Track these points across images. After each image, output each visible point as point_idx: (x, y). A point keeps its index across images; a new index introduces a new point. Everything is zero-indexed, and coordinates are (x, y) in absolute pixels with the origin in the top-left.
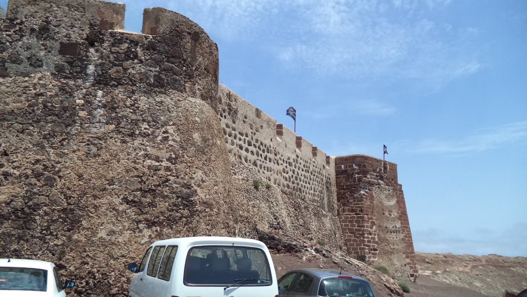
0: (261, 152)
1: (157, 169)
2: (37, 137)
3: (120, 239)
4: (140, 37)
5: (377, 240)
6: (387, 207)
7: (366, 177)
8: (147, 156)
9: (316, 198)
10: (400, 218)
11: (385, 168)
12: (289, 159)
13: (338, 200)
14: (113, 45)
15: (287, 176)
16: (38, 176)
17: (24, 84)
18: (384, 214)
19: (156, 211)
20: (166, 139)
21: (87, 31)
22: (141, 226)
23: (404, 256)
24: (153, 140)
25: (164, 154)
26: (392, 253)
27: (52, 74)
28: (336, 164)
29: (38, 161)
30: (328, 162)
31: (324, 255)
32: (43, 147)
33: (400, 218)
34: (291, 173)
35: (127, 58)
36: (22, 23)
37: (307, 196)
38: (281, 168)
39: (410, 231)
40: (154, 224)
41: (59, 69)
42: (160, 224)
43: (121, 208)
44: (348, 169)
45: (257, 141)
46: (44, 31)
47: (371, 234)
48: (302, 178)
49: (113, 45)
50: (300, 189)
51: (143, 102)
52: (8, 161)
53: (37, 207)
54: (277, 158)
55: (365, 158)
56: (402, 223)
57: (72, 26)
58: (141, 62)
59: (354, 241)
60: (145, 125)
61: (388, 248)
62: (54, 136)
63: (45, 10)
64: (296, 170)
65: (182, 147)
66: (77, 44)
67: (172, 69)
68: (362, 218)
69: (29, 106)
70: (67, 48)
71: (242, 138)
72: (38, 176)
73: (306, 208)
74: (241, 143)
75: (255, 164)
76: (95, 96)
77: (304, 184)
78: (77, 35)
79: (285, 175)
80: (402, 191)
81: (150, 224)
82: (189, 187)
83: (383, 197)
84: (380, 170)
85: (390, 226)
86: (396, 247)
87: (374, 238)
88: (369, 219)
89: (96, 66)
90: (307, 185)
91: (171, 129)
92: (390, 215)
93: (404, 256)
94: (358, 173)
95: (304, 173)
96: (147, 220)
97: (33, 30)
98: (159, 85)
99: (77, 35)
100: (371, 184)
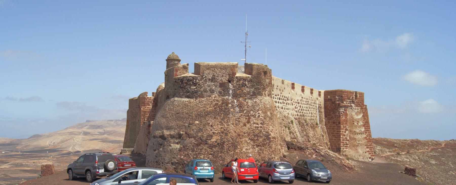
0: (284, 101)
1: (258, 128)
2: (220, 120)
3: (249, 151)
4: (246, 77)
5: (348, 139)
6: (356, 120)
7: (343, 103)
8: (254, 123)
9: (312, 118)
10: (364, 126)
11: (356, 96)
12: (298, 100)
13: (326, 116)
14: (237, 82)
16: (223, 133)
17: (210, 100)
18: (354, 124)
19: (259, 142)
20: (259, 116)
21: (228, 77)
22: (255, 147)
23: (366, 147)
24: (255, 117)
25: (259, 122)
26: (357, 146)
27: (218, 95)
28: (325, 95)
29: (222, 128)
30: (320, 95)
31: (316, 151)
32: (222, 123)
33: (364, 126)
34: (299, 108)
35: (243, 86)
36: (206, 77)
37: (307, 118)
38: (294, 106)
39: (370, 132)
40: (258, 146)
41: (220, 93)
42: (260, 146)
43: (248, 141)
44: (332, 98)
45: (283, 96)
46: (213, 80)
47: (345, 136)
48: (305, 109)
49: (237, 82)
51: (250, 102)
52: (213, 128)
53: (224, 143)
54: (292, 102)
55: (342, 92)
56: (365, 128)
57: (223, 76)
58: (248, 87)
59: (334, 139)
60: (252, 112)
61: (355, 143)
62: (225, 119)
63: (213, 71)
64: (302, 105)
65: (265, 118)
66: (225, 82)
67: (258, 87)
68: (340, 127)
69: (215, 109)
70: (222, 85)
71: (276, 97)
72: (223, 133)
73: (307, 125)
74: (276, 100)
75: (282, 108)
76: (234, 103)
77: (305, 112)
78: (225, 79)
79: (297, 110)
80: (367, 109)
81: (258, 146)
82: (267, 132)
83: (354, 114)
84: (353, 98)
85: (357, 131)
86: (360, 142)
87: (347, 138)
88: (344, 127)
89: (232, 90)
90: (308, 112)
91: (260, 112)
92: (358, 124)
93: (366, 147)
94: (338, 101)
95: (306, 106)
96: (256, 145)
97: (209, 79)
98: (254, 95)
99: (225, 79)
100: (346, 107)
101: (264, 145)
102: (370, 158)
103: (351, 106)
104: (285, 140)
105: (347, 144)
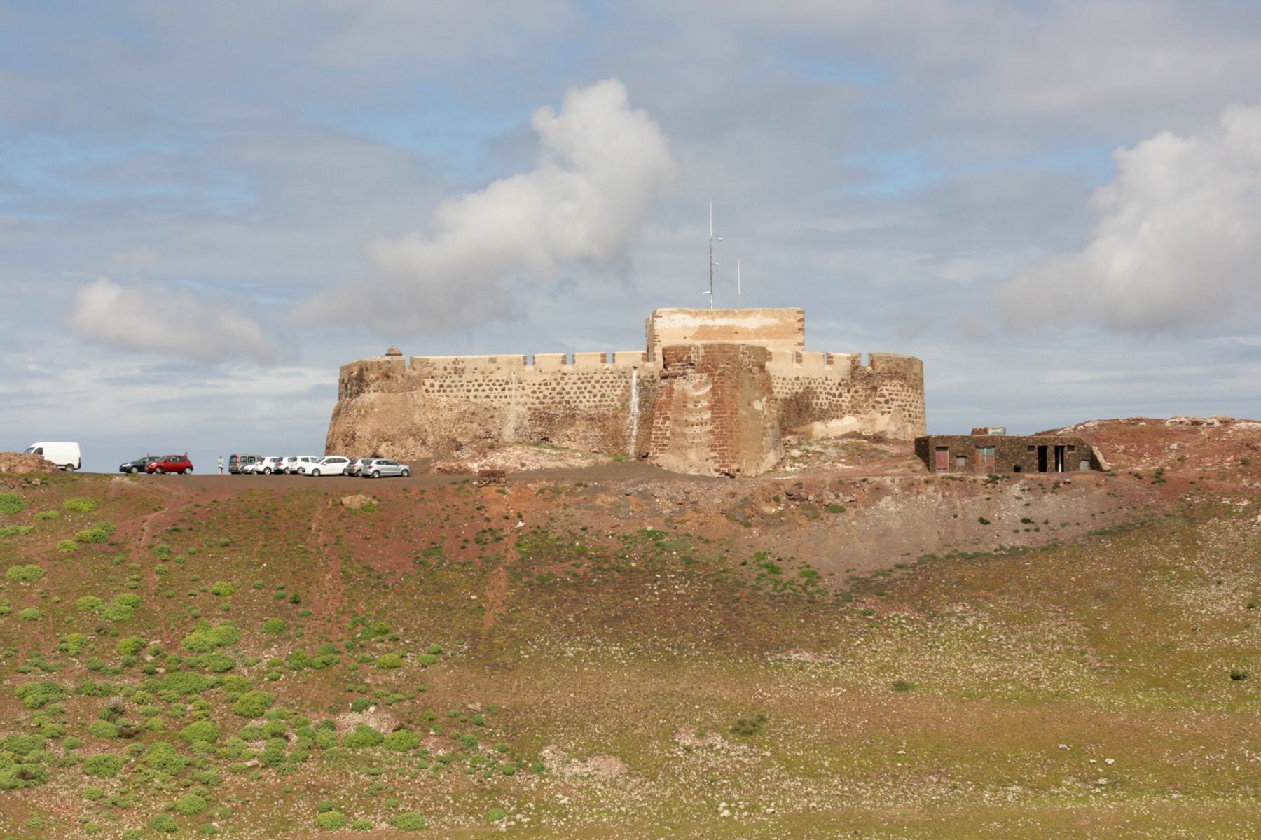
26: (687, 448)
50: (568, 402)
75: (487, 397)
85: (692, 419)
102: (716, 471)
103: (685, 374)
104: (454, 440)
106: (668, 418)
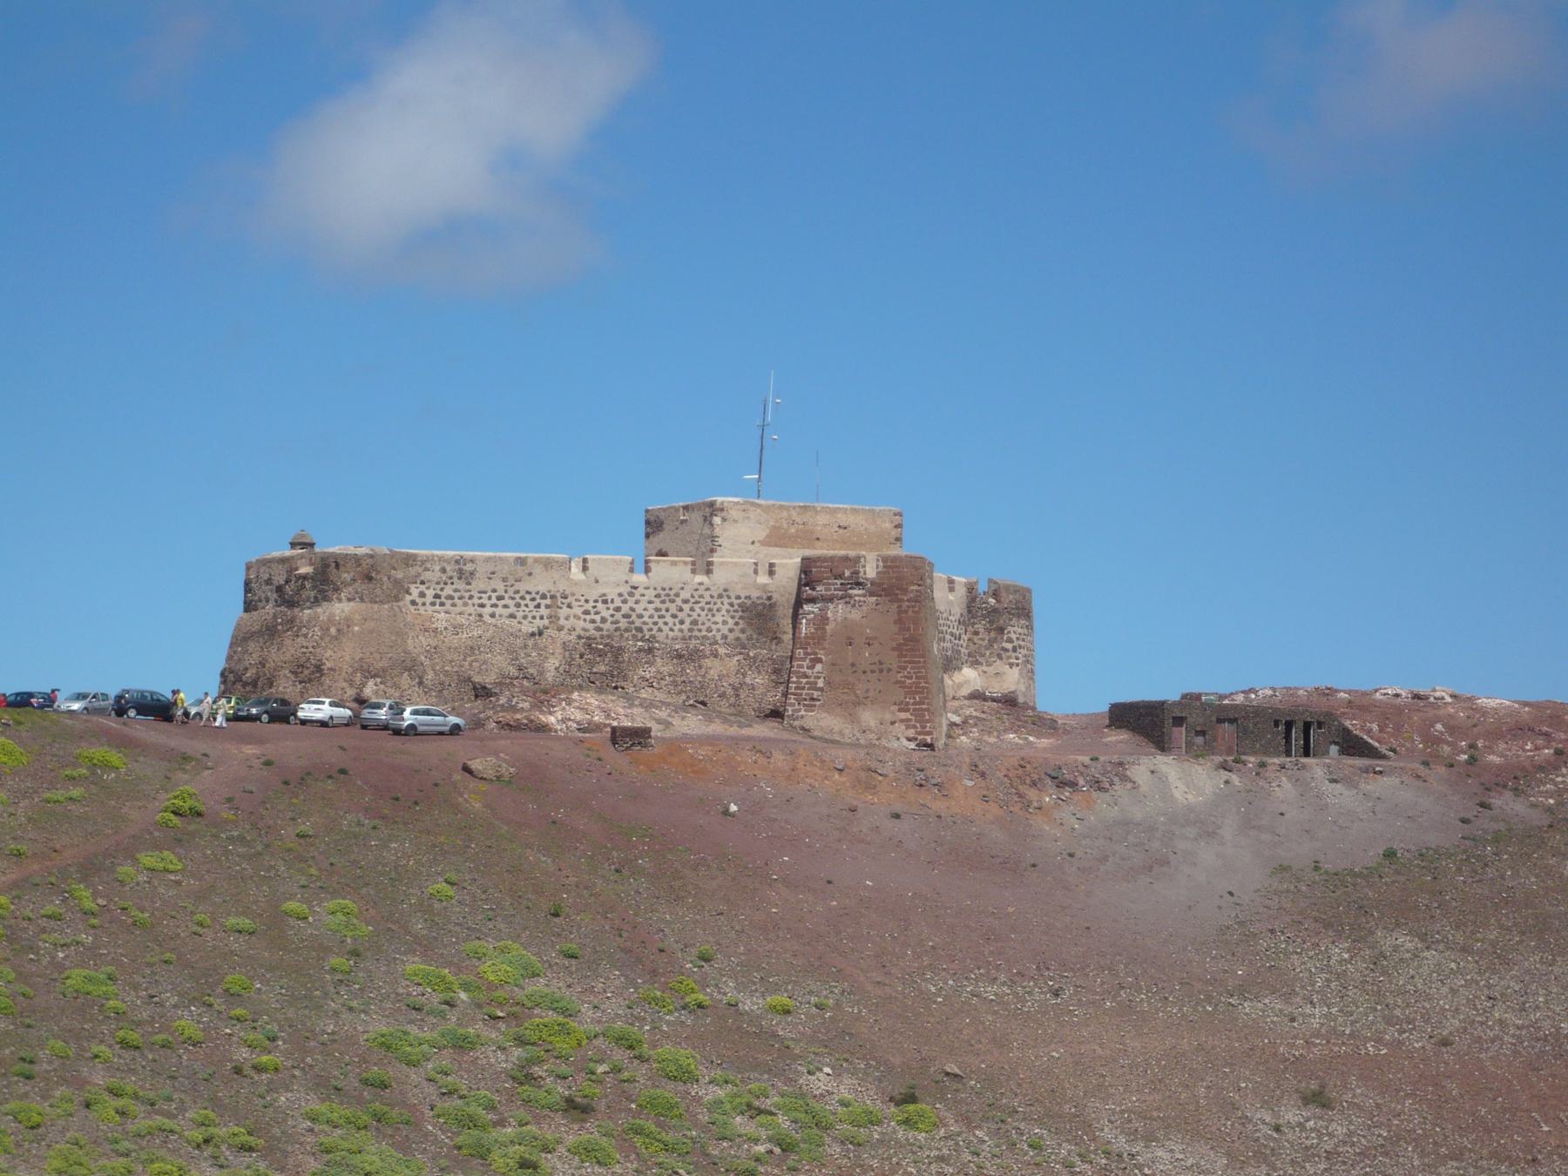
5: (820, 684)
15: (598, 618)
46: (269, 582)
50: (640, 630)
70: (279, 589)
75: (512, 616)
101: (310, 680)
104: (469, 679)
105: (813, 699)
106: (820, 661)
